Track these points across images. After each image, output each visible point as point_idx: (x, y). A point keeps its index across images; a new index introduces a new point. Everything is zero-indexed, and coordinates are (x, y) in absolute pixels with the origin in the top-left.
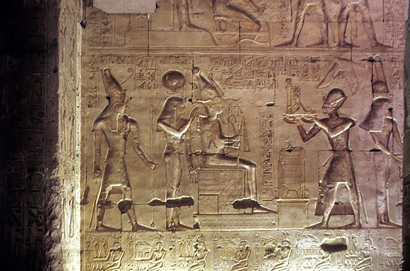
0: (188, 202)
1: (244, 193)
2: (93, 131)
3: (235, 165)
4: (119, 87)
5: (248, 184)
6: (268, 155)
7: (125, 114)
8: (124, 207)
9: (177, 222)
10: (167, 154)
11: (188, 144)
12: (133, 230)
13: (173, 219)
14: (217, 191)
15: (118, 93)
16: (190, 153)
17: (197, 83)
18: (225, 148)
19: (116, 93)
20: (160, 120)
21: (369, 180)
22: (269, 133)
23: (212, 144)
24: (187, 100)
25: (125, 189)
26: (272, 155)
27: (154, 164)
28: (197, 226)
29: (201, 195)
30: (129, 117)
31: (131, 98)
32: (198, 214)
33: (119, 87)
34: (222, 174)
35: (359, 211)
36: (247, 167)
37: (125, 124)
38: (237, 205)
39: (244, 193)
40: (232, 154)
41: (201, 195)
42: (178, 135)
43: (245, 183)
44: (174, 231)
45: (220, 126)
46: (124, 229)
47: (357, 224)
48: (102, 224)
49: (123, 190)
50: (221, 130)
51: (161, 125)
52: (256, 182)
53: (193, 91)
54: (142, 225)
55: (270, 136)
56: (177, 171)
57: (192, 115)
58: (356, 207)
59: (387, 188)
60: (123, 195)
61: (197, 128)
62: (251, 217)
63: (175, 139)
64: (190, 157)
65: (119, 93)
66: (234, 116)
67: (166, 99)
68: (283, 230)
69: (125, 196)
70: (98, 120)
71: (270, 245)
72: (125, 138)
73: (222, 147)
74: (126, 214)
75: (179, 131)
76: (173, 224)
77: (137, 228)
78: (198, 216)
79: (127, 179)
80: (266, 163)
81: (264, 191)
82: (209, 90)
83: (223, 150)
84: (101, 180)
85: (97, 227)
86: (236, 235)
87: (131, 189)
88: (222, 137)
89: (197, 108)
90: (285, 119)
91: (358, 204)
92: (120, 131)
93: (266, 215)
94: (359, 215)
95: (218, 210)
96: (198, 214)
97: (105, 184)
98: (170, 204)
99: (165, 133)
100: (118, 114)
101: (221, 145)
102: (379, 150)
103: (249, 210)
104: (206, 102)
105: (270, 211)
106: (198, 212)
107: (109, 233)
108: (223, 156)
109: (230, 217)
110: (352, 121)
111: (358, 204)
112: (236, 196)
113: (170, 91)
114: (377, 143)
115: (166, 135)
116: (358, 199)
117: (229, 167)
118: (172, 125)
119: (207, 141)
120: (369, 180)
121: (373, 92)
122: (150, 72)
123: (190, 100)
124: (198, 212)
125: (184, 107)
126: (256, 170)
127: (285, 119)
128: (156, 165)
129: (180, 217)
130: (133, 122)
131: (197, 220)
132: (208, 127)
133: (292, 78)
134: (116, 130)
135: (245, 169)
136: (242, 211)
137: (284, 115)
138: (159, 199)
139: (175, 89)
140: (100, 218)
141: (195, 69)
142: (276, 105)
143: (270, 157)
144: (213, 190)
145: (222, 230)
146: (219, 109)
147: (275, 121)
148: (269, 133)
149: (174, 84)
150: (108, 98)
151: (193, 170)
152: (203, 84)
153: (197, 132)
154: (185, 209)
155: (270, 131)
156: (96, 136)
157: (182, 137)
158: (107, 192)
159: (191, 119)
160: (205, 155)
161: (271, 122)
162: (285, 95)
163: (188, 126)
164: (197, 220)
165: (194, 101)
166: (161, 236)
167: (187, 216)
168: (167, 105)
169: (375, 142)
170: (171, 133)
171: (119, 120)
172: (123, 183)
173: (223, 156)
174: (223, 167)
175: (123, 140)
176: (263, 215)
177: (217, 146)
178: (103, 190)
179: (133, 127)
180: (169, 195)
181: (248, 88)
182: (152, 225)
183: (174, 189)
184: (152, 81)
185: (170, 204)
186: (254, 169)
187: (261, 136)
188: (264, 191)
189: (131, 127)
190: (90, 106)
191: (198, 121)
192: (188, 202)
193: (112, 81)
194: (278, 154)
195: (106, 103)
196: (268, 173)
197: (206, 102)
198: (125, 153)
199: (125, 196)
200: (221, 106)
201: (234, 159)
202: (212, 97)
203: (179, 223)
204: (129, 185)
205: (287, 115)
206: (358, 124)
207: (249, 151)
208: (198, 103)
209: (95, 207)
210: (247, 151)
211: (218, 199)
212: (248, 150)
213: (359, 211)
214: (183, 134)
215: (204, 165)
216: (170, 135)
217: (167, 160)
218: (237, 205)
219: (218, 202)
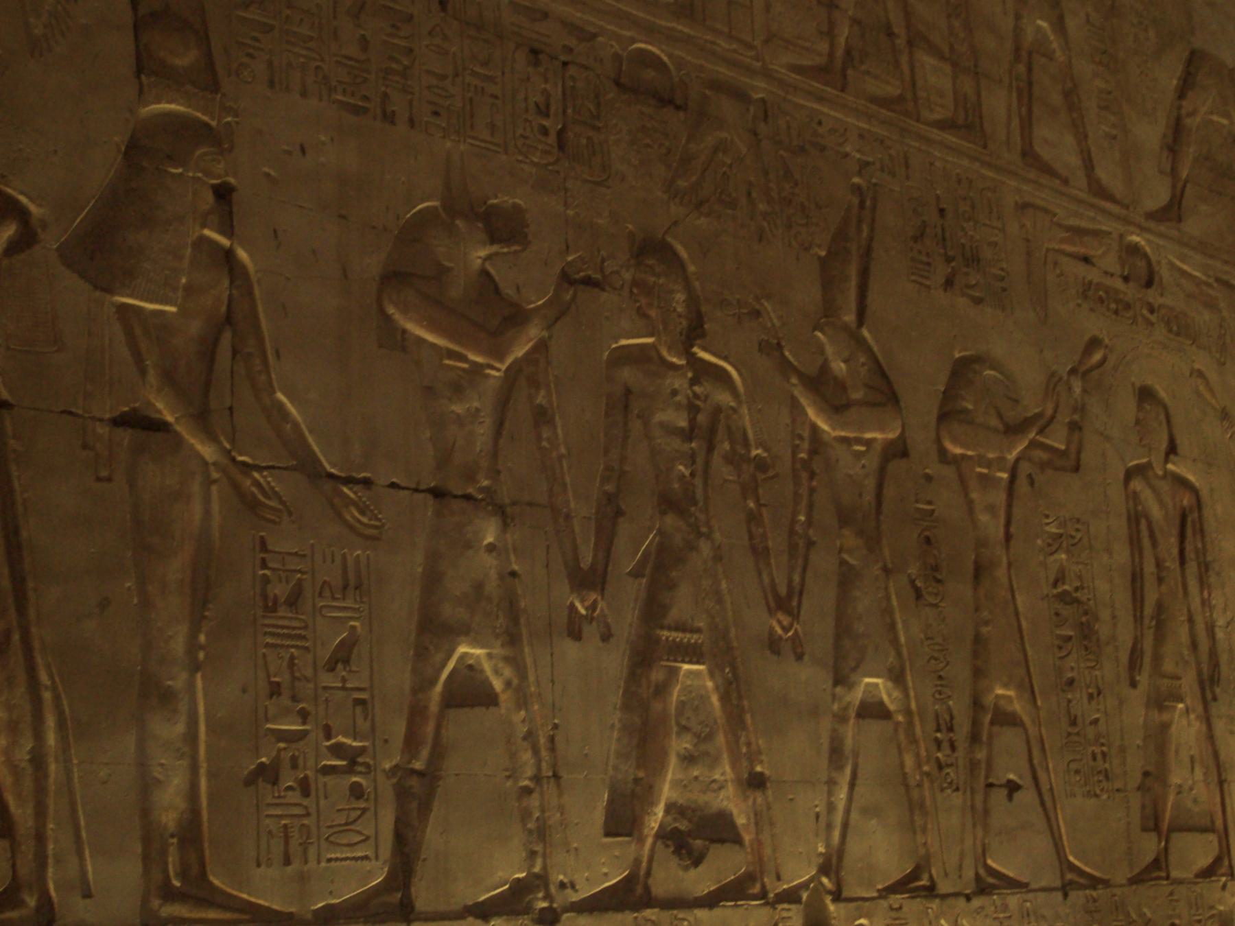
21: (104, 604)
35: (40, 812)
47: (32, 902)
58: (28, 784)
59: (195, 667)
91: (38, 761)
94: (40, 837)
102: (159, 426)
110: (22, 215)
111: (38, 761)
114: (152, 377)
116: (39, 736)
120: (104, 604)
121: (139, 70)
169: (143, 372)
206: (50, 241)
213: (40, 812)
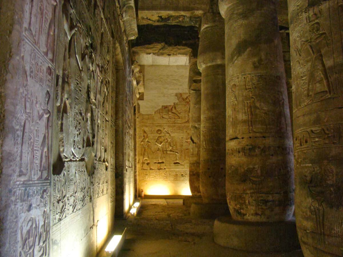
0: (163, 163)
4: (146, 133)
8: (148, 164)
10: (158, 150)
19: (145, 135)
20: (156, 142)
28: (165, 169)
36: (177, 154)
38: (175, 163)
42: (160, 146)
51: (156, 143)
55: (182, 146)
62: (177, 166)
63: (160, 146)
64: (163, 151)
68: (185, 169)
70: (141, 142)
71: (182, 173)
72: (148, 146)
73: (171, 149)
75: (160, 144)
77: (151, 169)
86: (174, 171)
88: (171, 146)
92: (147, 144)
98: (159, 163)
101: (170, 148)
103: (177, 165)
105: (182, 165)
108: (171, 151)
115: (158, 146)
119: (167, 147)
130: (150, 142)
132: (167, 143)
136: (175, 165)
139: (160, 134)
140: (142, 167)
141: (164, 129)
146: (170, 139)
150: (144, 136)
152: (166, 132)
154: (162, 164)
160: (166, 151)
164: (165, 167)
167: (163, 166)
173: (171, 151)
178: (143, 160)
179: (150, 144)
180: (158, 161)
185: (159, 163)
190: (140, 138)
192: (163, 163)
193: (145, 132)
195: (143, 138)
201: (173, 152)
204: (149, 158)
215: (167, 153)
217: (158, 152)
218: (175, 163)
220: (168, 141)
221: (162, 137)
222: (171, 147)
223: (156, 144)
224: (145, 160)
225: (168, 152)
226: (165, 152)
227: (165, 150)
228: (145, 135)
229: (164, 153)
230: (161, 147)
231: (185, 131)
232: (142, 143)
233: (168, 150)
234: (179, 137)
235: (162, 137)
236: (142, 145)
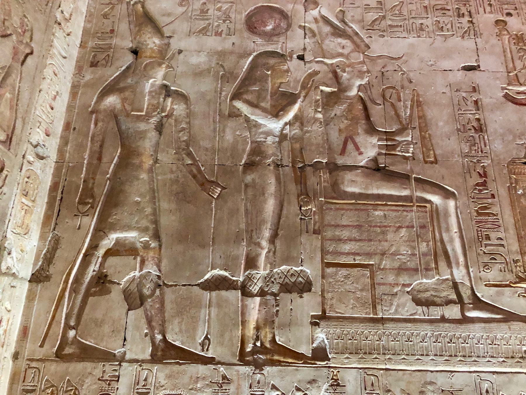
1: (436, 263)
2: (92, 112)
3: (405, 193)
4: (158, 30)
5: (442, 241)
6: (481, 172)
7: (165, 82)
9: (269, 337)
10: (250, 166)
11: (297, 146)
12: (155, 359)
13: (258, 328)
14: (369, 255)
15: (154, 43)
16: (301, 165)
17: (314, 27)
18: (379, 154)
20: (236, 96)
22: (475, 124)
23: (350, 146)
24: (295, 56)
25: (146, 246)
26: (491, 172)
27: (218, 185)
29: (329, 265)
30: (172, 88)
31: (180, 52)
32: (324, 317)
33: (158, 30)
34: (377, 213)
36: (436, 199)
37: (162, 100)
39: (436, 263)
40: (398, 168)
41: (329, 265)
42: (275, 126)
43: (434, 238)
44: (259, 366)
45: (365, 108)
46: (128, 357)
48: (75, 337)
49: (139, 245)
50: (368, 117)
51: (239, 104)
52: (462, 237)
53: (307, 40)
54: (177, 344)
56: (270, 206)
57: (303, 87)
60: (139, 259)
61: (316, 111)
62: (462, 331)
63: (268, 133)
64: (300, 175)
65: (157, 41)
66: (394, 88)
67: (250, 54)
69: (143, 262)
72: (160, 128)
73: (370, 153)
74: (140, 311)
75: (276, 114)
76: (258, 344)
77: (166, 353)
78: (322, 323)
79: (156, 222)
80: (480, 191)
81: (486, 259)
82: (340, 40)
83: (375, 160)
84: (91, 223)
85: (61, 347)
87: (160, 246)
88: (372, 130)
89: (316, 73)
90: (507, 96)
93: (504, 326)
95: (374, 307)
96: (324, 317)
97: (101, 231)
99: (247, 120)
100: (151, 81)
101: (370, 148)
104: (334, 61)
106: (324, 311)
107: (88, 366)
109: (408, 329)
112: (416, 270)
113: (259, 41)
117: (391, 198)
118: (263, 104)
119: (336, 139)
122: (221, 7)
123: (301, 58)
124: (324, 311)
125: (288, 71)
126: (456, 208)
127: (507, 96)
128: (223, 188)
129: (276, 324)
131: (321, 335)
132: (339, 109)
133: (507, 19)
134: (142, 112)
135: (429, 202)
137: (503, 89)
138: (226, 274)
139: (270, 36)
142: (481, 68)
143: (485, 175)
144: (358, 254)
145: (388, 367)
146: (361, 74)
147: (486, 100)
148: (475, 124)
149: (269, 28)
150: (135, 52)
151: (307, 203)
152: (327, 29)
153: (316, 120)
155: (478, 120)
156: (96, 124)
157: (283, 129)
158: (101, 252)
159: (303, 94)
160: (333, 168)
161: (476, 102)
162: (499, 50)
163: (296, 107)
164: (321, 335)
165: (307, 58)
166: (224, 377)
168: (253, 66)
170: (261, 121)
171: (150, 92)
172: (144, 230)
174: (379, 197)
175: (153, 135)
176: (493, 325)
177: (362, 150)
181: (419, 37)
182: (202, 344)
183: (262, 248)
184: (224, 21)
186: (451, 203)
187: (458, 130)
188: (486, 259)
189: (175, 107)
190: (94, 64)
191: (318, 98)
194: (505, 171)
196: (488, 214)
197: (334, 61)
198: (156, 161)
199: (143, 262)
200: (365, 68)
201: (403, 178)
202: (346, 52)
203: (273, 340)
204: (157, 236)
205: (510, 88)
207: (436, 162)
208: (317, 62)
209: (64, 290)
210: (432, 163)
211: (372, 277)
212: (432, 159)
214: (286, 124)
215: (335, 191)
216: (257, 125)
217: (249, 178)
219: (373, 285)
220: (342, 89)
221: (294, 64)
222: (374, 140)
223: (235, 114)
224: (109, 253)
225: (353, 184)
226: (319, 180)
227: (317, 166)
228: (152, 42)
229: (305, 194)
230: (283, 137)
231: (486, 19)
232: (112, 100)
233: (341, 161)
234: (446, 64)
235: (294, 64)
236: (114, 115)
